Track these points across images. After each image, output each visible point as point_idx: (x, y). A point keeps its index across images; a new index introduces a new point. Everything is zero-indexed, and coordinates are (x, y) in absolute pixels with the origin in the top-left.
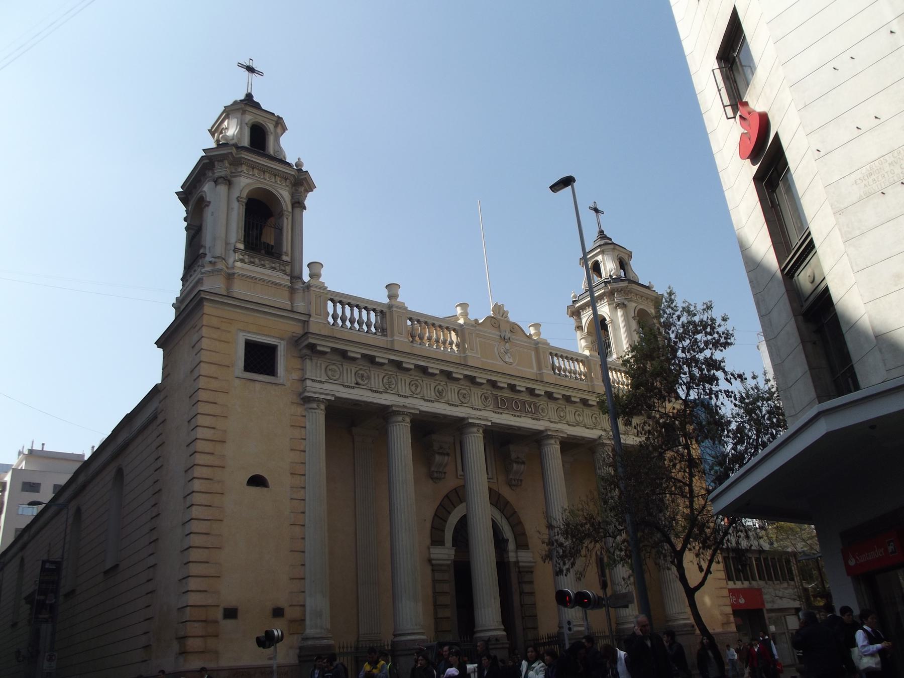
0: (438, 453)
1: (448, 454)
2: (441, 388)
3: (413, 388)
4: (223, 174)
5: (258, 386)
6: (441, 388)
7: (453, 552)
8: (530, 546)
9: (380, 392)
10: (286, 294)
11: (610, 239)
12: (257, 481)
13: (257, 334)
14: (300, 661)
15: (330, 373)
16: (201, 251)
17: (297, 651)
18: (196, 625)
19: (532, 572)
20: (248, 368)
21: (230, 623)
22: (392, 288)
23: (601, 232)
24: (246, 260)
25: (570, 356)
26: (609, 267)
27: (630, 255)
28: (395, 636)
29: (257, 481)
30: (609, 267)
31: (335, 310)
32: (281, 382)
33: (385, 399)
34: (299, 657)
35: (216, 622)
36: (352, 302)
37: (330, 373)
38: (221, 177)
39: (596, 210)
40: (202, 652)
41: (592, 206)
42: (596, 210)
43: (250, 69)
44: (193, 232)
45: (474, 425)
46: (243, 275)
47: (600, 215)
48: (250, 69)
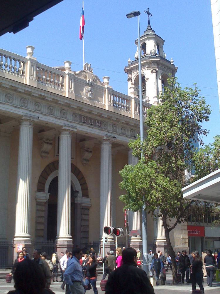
1: (51, 144)
3: (37, 107)
7: (48, 195)
8: (89, 196)
9: (18, 108)
11: (154, 31)
19: (89, 209)
25: (123, 97)
26: (151, 46)
27: (163, 42)
30: (151, 46)
39: (149, 13)
42: (149, 13)
45: (65, 130)
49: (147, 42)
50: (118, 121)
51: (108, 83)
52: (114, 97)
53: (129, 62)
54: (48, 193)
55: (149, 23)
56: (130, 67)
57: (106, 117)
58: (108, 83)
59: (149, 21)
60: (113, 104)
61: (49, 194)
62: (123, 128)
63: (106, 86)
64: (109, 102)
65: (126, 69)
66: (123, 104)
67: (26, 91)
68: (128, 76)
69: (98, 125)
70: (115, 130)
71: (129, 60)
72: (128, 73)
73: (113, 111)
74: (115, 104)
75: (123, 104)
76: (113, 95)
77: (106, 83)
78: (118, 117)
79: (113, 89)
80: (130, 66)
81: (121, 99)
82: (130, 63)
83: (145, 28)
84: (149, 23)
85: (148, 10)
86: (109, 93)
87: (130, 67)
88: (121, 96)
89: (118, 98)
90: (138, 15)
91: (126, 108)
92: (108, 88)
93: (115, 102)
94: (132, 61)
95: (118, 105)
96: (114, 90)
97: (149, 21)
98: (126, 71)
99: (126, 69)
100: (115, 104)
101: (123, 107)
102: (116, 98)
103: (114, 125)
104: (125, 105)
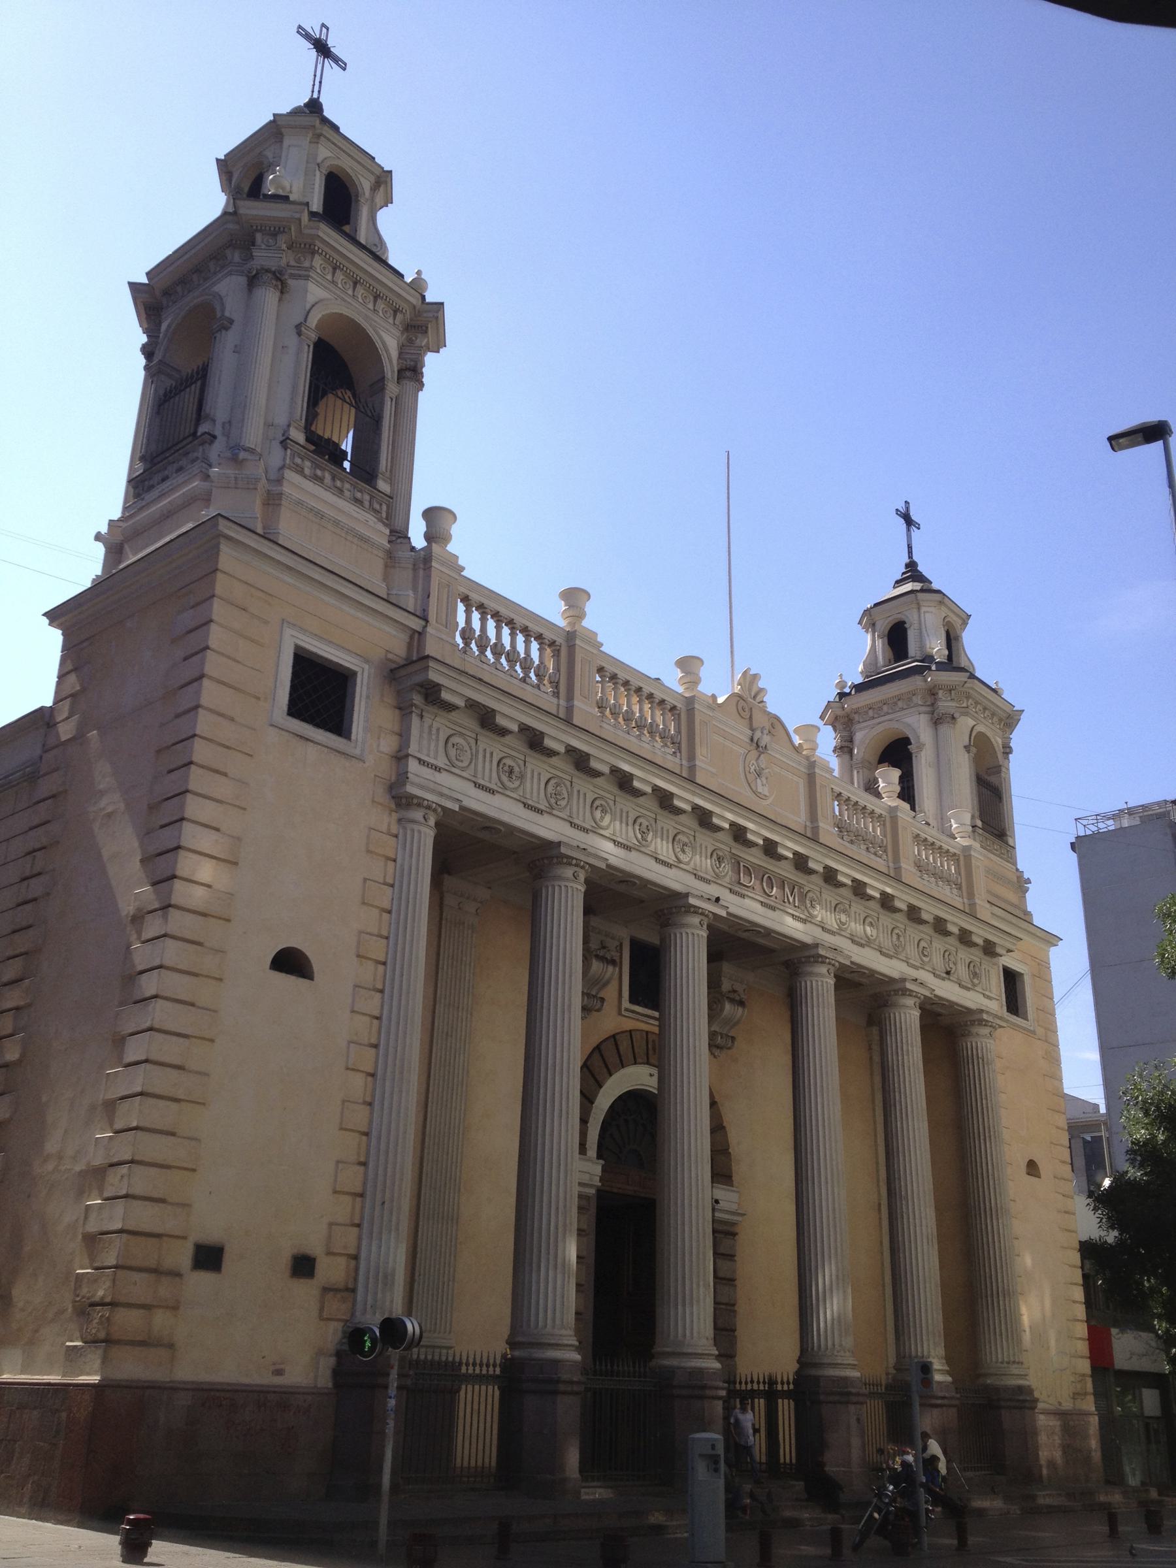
0: (597, 956)
1: (613, 962)
2: (645, 823)
4: (273, 265)
5: (311, 749)
6: (645, 823)
7: (597, 1169)
9: (540, 811)
10: (379, 565)
12: (290, 962)
13: (320, 638)
14: (336, 1385)
15: (452, 752)
16: (203, 428)
17: (332, 1361)
18: (136, 1276)
19: (734, 1234)
20: (297, 709)
21: (205, 1278)
22: (574, 598)
23: (911, 566)
24: (307, 471)
27: (965, 618)
28: (512, 1344)
29: (290, 962)
31: (468, 620)
32: (357, 752)
33: (547, 828)
34: (336, 1373)
35: (176, 1274)
36: (504, 611)
37: (452, 752)
38: (268, 271)
40: (143, 1344)
41: (902, 507)
43: (322, 48)
44: (169, 383)
45: (696, 910)
46: (300, 503)
47: (915, 533)
48: (322, 48)
49: (911, 617)
54: (599, 1156)
55: (910, 557)
59: (910, 547)
61: (602, 1162)
69: (791, 900)
83: (899, 570)
84: (910, 557)
85: (908, 509)
97: (910, 547)
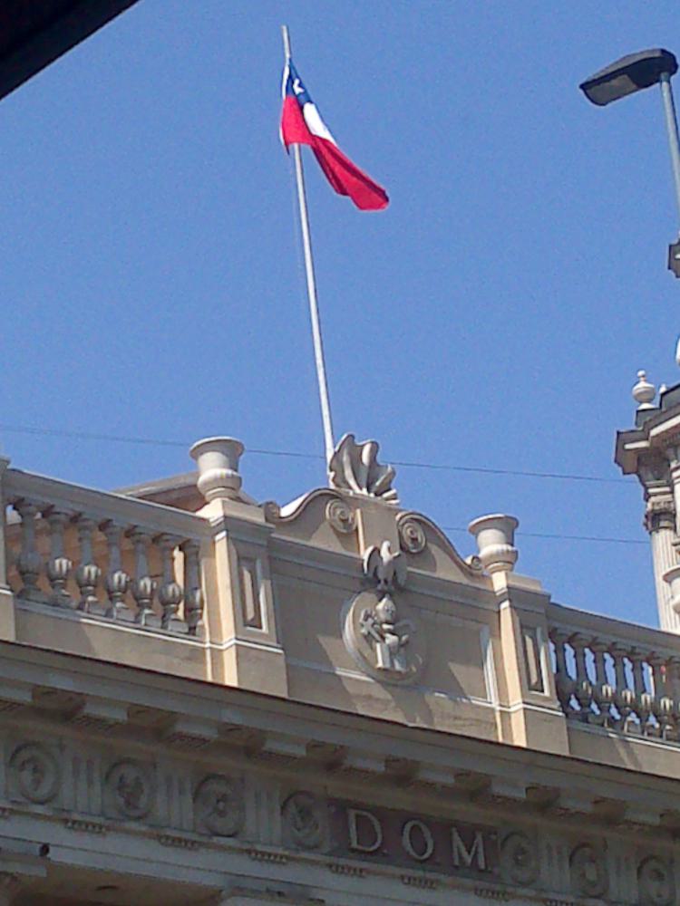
25: (624, 644)
50: (611, 816)
51: (509, 561)
52: (560, 651)
53: (640, 398)
56: (654, 432)
57: (522, 795)
58: (509, 561)
60: (565, 705)
62: (653, 864)
63: (499, 582)
64: (531, 686)
65: (628, 446)
66: (629, 694)
67: (38, 692)
68: (647, 497)
70: (593, 884)
71: (642, 385)
72: (642, 472)
73: (566, 753)
74: (574, 703)
75: (629, 694)
76: (552, 635)
77: (493, 558)
78: (607, 792)
79: (549, 597)
80: (649, 426)
81: (610, 661)
82: (649, 401)
86: (522, 627)
87: (654, 432)
88: (606, 639)
89: (590, 657)
90: (663, 76)
91: (652, 720)
92: (512, 593)
93: (568, 687)
94: (663, 389)
95: (594, 706)
96: (552, 600)
98: (631, 464)
99: (628, 446)
100: (574, 703)
101: (633, 717)
102: (579, 656)
103: (579, 852)
104: (648, 698)
